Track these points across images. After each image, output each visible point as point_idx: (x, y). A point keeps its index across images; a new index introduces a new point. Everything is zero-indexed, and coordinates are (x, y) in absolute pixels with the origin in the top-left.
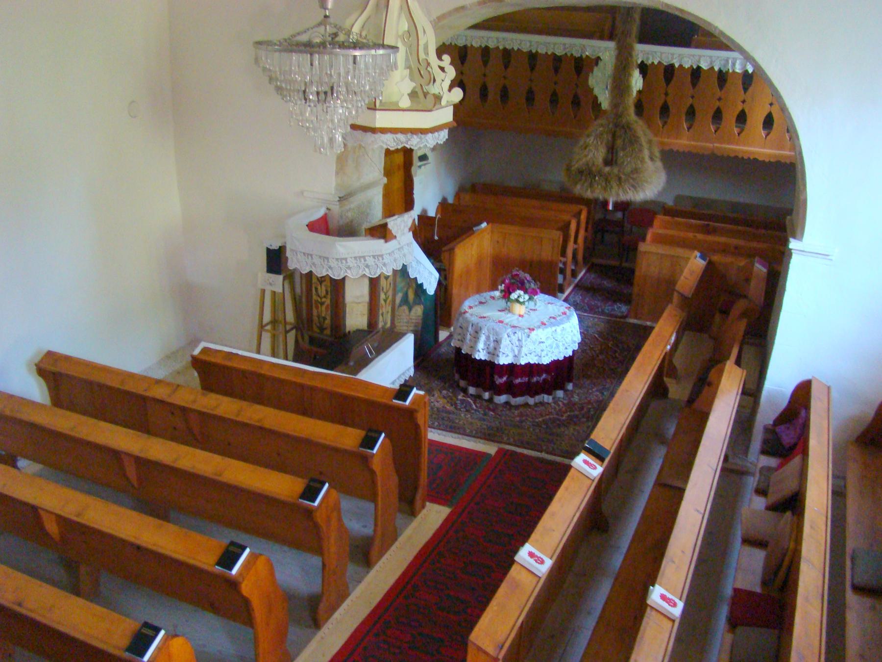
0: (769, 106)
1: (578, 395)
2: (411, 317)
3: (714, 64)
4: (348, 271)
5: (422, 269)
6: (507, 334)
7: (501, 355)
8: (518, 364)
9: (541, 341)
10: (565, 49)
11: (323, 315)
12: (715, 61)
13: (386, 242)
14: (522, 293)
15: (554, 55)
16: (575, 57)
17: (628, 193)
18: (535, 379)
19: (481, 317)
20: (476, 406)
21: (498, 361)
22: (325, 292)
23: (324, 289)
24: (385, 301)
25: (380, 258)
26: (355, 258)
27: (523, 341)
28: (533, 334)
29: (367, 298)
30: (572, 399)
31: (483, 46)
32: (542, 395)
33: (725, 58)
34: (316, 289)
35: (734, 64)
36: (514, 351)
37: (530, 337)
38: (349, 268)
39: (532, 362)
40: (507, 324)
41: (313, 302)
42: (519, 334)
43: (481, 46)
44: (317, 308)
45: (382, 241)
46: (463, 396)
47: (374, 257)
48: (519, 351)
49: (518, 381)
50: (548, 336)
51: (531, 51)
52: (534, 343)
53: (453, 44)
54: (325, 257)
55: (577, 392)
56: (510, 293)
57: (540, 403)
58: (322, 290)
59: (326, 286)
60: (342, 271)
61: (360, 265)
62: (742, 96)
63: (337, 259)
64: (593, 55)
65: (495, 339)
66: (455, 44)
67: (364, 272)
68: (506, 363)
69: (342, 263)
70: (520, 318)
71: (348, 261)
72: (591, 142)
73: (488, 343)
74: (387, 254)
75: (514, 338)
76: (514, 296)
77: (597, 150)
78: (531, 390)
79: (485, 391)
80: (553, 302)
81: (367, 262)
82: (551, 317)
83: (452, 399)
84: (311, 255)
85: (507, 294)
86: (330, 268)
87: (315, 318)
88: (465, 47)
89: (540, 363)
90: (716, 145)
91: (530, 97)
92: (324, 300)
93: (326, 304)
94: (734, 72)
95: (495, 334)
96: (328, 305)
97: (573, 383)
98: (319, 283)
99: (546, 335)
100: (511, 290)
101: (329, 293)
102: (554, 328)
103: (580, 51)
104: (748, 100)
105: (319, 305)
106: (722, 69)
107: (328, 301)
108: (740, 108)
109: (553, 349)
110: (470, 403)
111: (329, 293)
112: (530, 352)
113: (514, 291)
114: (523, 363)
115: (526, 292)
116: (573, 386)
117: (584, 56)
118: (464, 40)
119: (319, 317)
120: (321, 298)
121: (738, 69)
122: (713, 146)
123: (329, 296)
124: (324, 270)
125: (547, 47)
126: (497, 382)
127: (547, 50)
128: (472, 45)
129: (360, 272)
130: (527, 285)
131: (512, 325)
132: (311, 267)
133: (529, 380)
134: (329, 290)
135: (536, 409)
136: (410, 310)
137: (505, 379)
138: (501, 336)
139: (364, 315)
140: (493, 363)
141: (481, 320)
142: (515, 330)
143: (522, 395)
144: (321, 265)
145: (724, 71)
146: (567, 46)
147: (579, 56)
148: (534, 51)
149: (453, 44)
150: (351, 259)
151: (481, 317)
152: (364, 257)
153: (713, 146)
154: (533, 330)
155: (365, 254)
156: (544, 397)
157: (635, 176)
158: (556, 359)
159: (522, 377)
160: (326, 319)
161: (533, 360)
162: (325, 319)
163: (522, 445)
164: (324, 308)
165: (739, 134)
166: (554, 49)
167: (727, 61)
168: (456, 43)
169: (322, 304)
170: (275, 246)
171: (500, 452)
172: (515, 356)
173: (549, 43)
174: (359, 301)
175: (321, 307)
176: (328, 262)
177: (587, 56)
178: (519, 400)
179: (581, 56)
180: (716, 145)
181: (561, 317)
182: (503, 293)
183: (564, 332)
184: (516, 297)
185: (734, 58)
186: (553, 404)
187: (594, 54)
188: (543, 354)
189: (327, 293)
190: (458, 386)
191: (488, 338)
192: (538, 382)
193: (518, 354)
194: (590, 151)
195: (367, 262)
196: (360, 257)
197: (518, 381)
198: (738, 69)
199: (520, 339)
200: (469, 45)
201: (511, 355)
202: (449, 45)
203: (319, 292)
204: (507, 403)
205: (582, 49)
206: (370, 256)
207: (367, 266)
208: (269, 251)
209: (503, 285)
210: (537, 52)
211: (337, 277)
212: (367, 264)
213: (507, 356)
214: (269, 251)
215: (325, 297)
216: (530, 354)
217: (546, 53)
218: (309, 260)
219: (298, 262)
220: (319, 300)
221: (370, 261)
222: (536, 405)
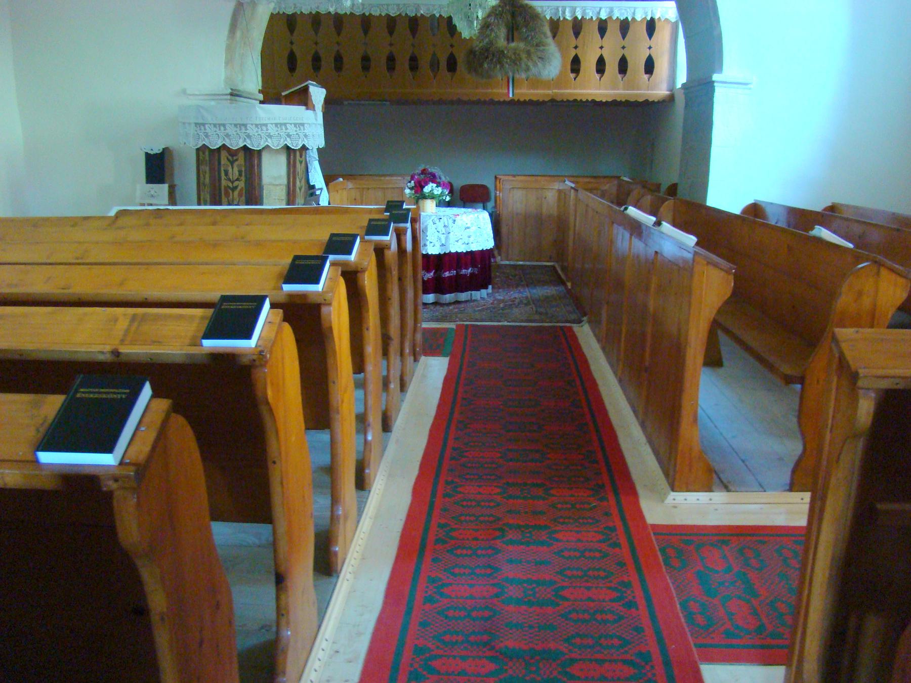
0: (600, 50)
3: (546, 13)
4: (269, 140)
7: (428, 243)
8: (447, 252)
10: (399, 9)
12: (546, 11)
13: (307, 109)
14: (435, 185)
15: (388, 16)
16: (410, 16)
17: (537, 64)
18: (464, 271)
21: (426, 251)
22: (237, 173)
23: (236, 169)
24: (300, 189)
25: (302, 128)
26: (276, 125)
27: (450, 226)
28: (458, 219)
29: (285, 181)
31: (314, 12)
32: (470, 292)
33: (556, 8)
35: (564, 12)
36: (440, 239)
37: (456, 222)
38: (270, 136)
41: (223, 188)
42: (444, 220)
43: (311, 13)
45: (304, 108)
47: (295, 125)
48: (447, 238)
49: (447, 274)
51: (364, 14)
53: (281, 13)
54: (240, 124)
56: (422, 187)
58: (234, 172)
59: (239, 166)
60: (263, 140)
61: (281, 134)
62: (573, 42)
63: (257, 125)
64: (427, 14)
66: (284, 13)
67: (286, 142)
68: (434, 253)
69: (262, 130)
71: (269, 128)
72: (492, 21)
74: (307, 124)
75: (440, 225)
76: (427, 189)
77: (499, 29)
78: (460, 285)
81: (288, 131)
84: (224, 125)
85: (419, 188)
86: (249, 136)
88: (294, 15)
90: (554, 91)
91: (366, 62)
92: (236, 183)
93: (239, 188)
94: (564, 18)
96: (241, 190)
98: (229, 164)
100: (423, 184)
101: (243, 174)
102: (476, 215)
103: (414, 10)
104: (580, 45)
105: (231, 192)
106: (553, 18)
107: (241, 184)
108: (573, 54)
111: (243, 174)
112: (457, 240)
113: (427, 184)
114: (453, 251)
116: (493, 288)
117: (419, 15)
118: (293, 8)
120: (232, 182)
121: (568, 17)
122: (552, 92)
123: (243, 178)
124: (241, 140)
125: (380, 9)
127: (380, 11)
128: (302, 12)
129: (282, 140)
130: (438, 180)
132: (224, 139)
133: (457, 273)
134: (243, 169)
137: (432, 274)
138: (425, 224)
139: (282, 200)
143: (450, 293)
144: (237, 134)
145: (555, 20)
146: (401, 6)
147: (414, 15)
148: (367, 14)
149: (281, 13)
150: (271, 125)
152: (285, 124)
153: (552, 92)
154: (458, 215)
155: (285, 122)
156: (471, 294)
157: (542, 48)
159: (449, 270)
161: (460, 248)
163: (477, 320)
164: (236, 193)
165: (575, 79)
166: (387, 10)
167: (557, 9)
168: (285, 12)
170: (157, 149)
171: (457, 326)
172: (443, 245)
173: (382, 5)
174: (277, 183)
175: (233, 192)
176: (246, 129)
177: (422, 15)
178: (448, 297)
179: (416, 15)
180: (554, 91)
182: (413, 192)
184: (430, 189)
185: (563, 7)
187: (428, 12)
188: (471, 240)
189: (240, 175)
193: (445, 243)
194: (492, 30)
195: (288, 131)
196: (281, 124)
197: (447, 274)
198: (568, 17)
199: (446, 224)
200: (299, 13)
201: (438, 244)
202: (276, 14)
204: (435, 304)
205: (416, 9)
206: (291, 124)
207: (289, 136)
208: (148, 157)
209: (413, 182)
210: (370, 14)
211: (257, 147)
212: (289, 133)
214: (148, 157)
215: (238, 180)
216: (457, 241)
217: (380, 14)
219: (207, 136)
220: (230, 185)
221: (292, 130)
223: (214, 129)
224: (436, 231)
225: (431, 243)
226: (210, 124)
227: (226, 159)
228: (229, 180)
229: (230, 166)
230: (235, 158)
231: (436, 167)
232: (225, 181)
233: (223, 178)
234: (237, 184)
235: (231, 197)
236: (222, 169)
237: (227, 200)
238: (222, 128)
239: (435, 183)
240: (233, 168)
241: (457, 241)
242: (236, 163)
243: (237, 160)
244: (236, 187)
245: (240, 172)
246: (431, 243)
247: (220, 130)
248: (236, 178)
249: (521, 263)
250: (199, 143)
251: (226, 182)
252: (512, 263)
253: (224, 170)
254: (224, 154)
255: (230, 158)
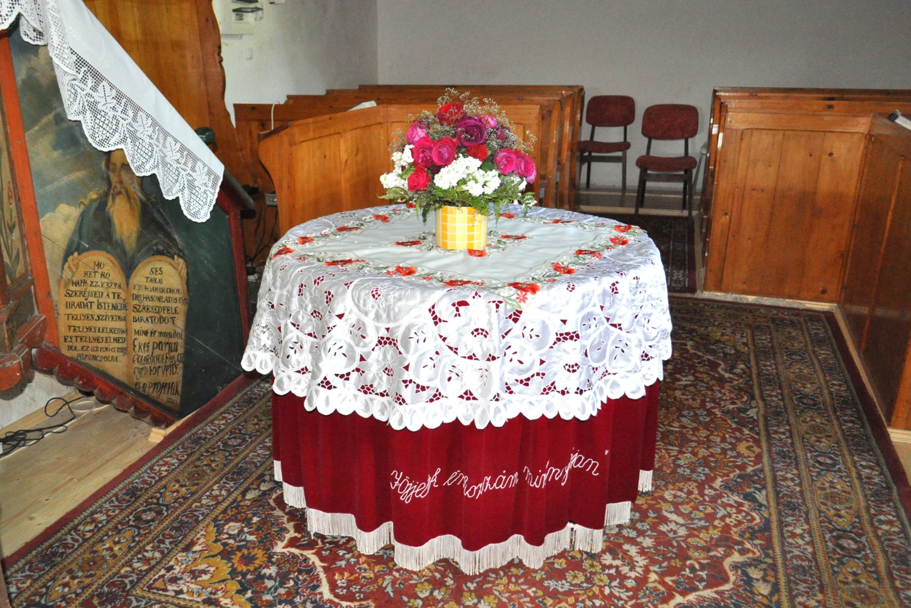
1: (676, 507)
2: (135, 292)
5: (144, 130)
6: (432, 310)
9: (566, 329)
14: (478, 163)
19: (334, 263)
20: (333, 586)
21: (401, 421)
28: (532, 305)
30: (663, 528)
37: (522, 318)
39: (532, 415)
40: (427, 277)
46: (293, 543)
49: (485, 485)
50: (588, 309)
52: (538, 337)
55: (668, 495)
57: (562, 555)
65: (383, 333)
68: (433, 424)
70: (475, 259)
73: (359, 351)
76: (445, 179)
79: (366, 525)
80: (566, 219)
82: (580, 252)
83: (248, 560)
89: (566, 417)
95: (384, 316)
97: (655, 470)
99: (583, 307)
102: (607, 282)
109: (606, 360)
110: (310, 570)
112: (523, 377)
115: (488, 163)
116: (655, 478)
126: (406, 497)
131: (447, 280)
133: (522, 476)
135: (552, 584)
136: (128, 268)
137: (432, 480)
140: (384, 427)
141: (331, 269)
142: (458, 294)
151: (334, 263)
154: (533, 289)
158: (616, 395)
181: (614, 251)
183: (639, 297)
186: (608, 559)
190: (280, 501)
191: (359, 331)
192: (553, 484)
197: (485, 485)
213: (437, 396)
216: (526, 382)
222: (551, 570)
224: (444, 344)
225: (423, 389)
231: (486, 100)
239: (475, 156)
241: (526, 382)
246: (423, 389)
249: (751, 299)
252: (730, 297)
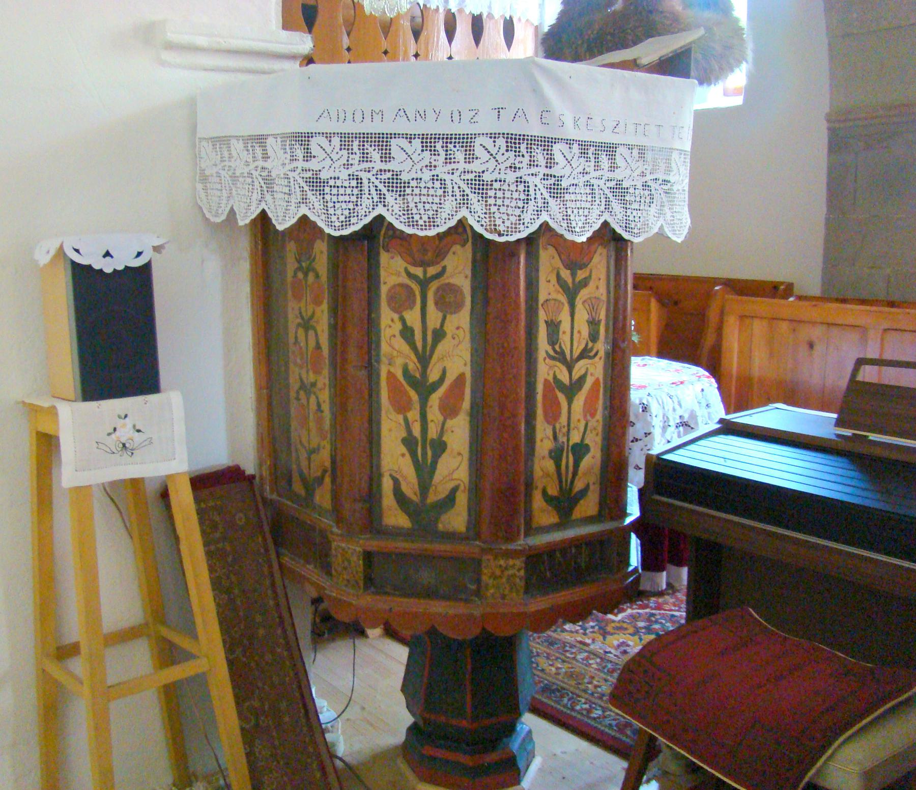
11: (575, 438)
23: (582, 315)
34: (553, 327)
41: (540, 388)
44: (552, 415)
59: (592, 303)
87: (543, 465)
93: (589, 381)
98: (563, 298)
105: (562, 398)
119: (556, 455)
120: (570, 369)
160: (587, 449)
162: (580, 450)
164: (579, 401)
169: (571, 390)
175: (570, 401)
189: (594, 337)
203: (565, 339)
215: (584, 354)
218: (602, 178)
219: (556, 190)
220: (564, 377)
223: (579, 164)
226: (569, 142)
227: (554, 280)
228: (560, 356)
229: (566, 308)
230: (581, 275)
232: (547, 360)
233: (541, 355)
234: (583, 372)
235: (563, 419)
236: (542, 316)
237: (549, 432)
238: (605, 162)
240: (572, 315)
242: (584, 294)
243: (585, 283)
244: (582, 379)
245: (593, 323)
247: (597, 167)
248: (582, 347)
250: (527, 217)
251: (551, 367)
253: (546, 322)
254: (548, 259)
255: (566, 274)
